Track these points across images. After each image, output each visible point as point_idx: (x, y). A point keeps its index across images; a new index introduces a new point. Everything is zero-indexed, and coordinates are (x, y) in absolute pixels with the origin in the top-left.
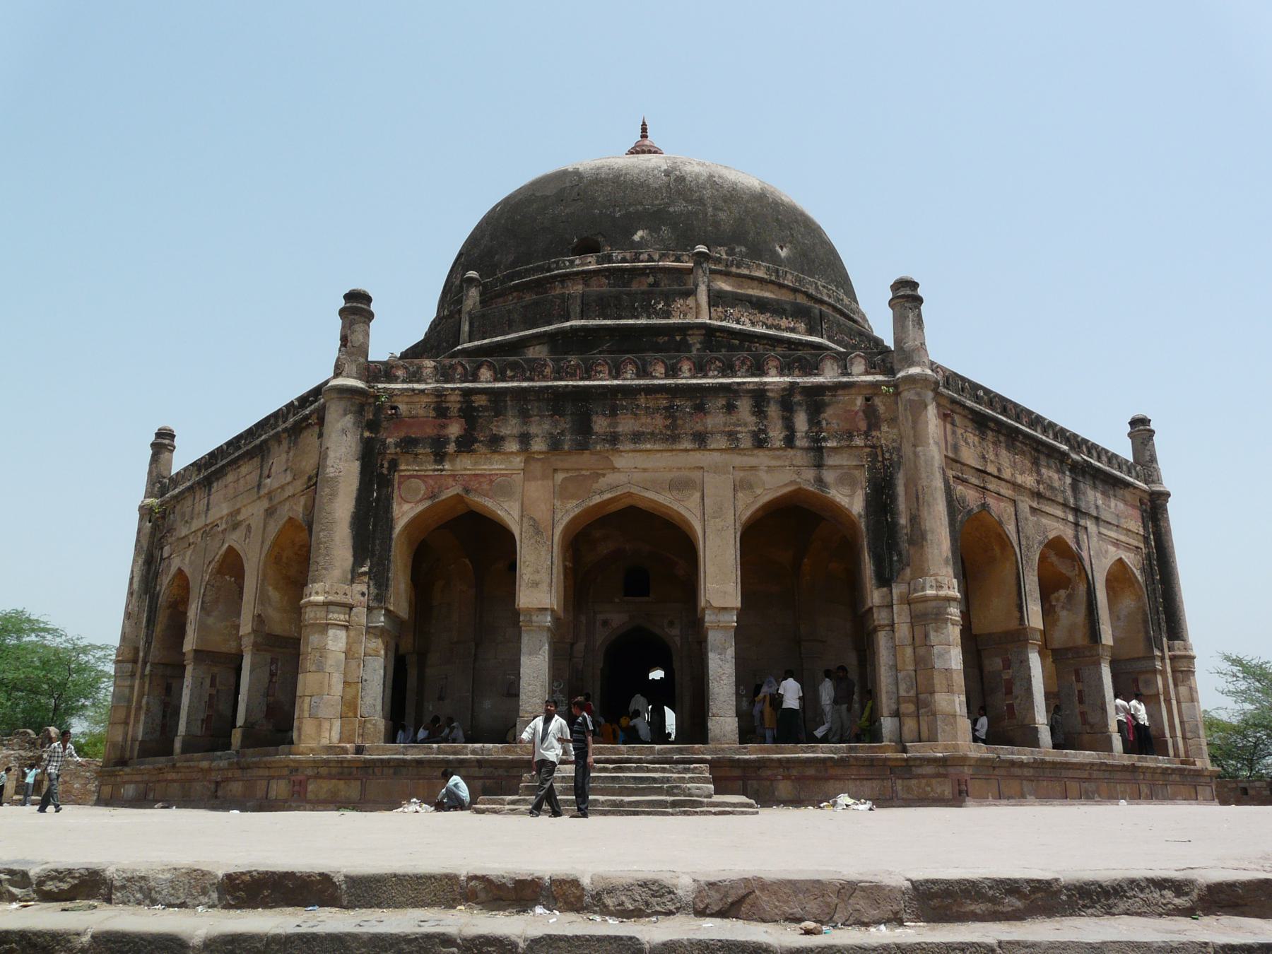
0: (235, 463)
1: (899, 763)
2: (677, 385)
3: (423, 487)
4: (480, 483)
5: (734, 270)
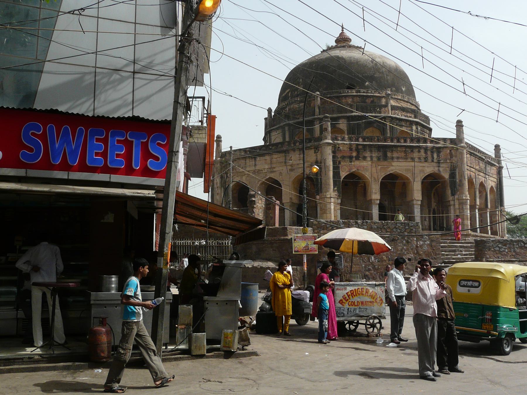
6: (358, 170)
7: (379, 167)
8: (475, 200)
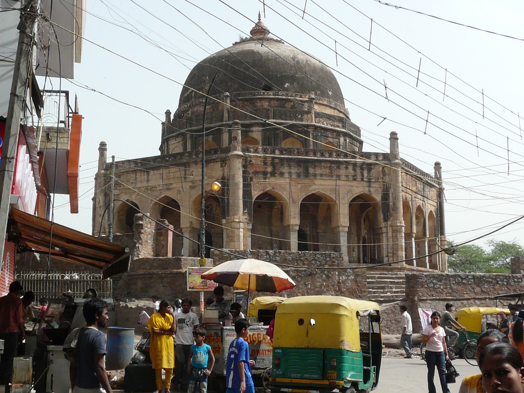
6: (273, 188)
7: (300, 186)
8: (411, 227)
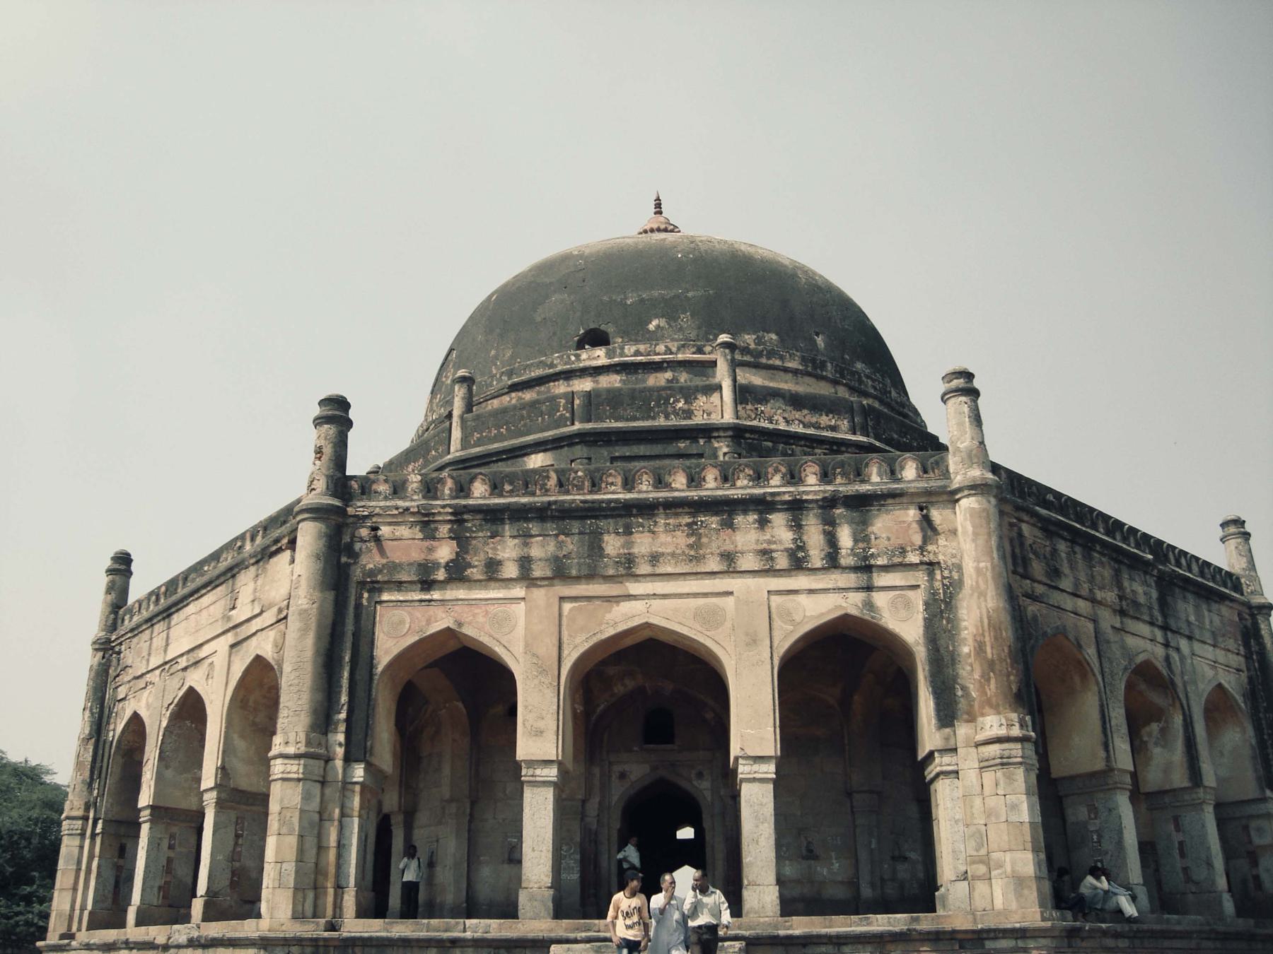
0: (195, 593)
1: (970, 936)
2: (701, 497)
3: (408, 620)
4: (474, 615)
5: (764, 360)
6: (460, 625)
